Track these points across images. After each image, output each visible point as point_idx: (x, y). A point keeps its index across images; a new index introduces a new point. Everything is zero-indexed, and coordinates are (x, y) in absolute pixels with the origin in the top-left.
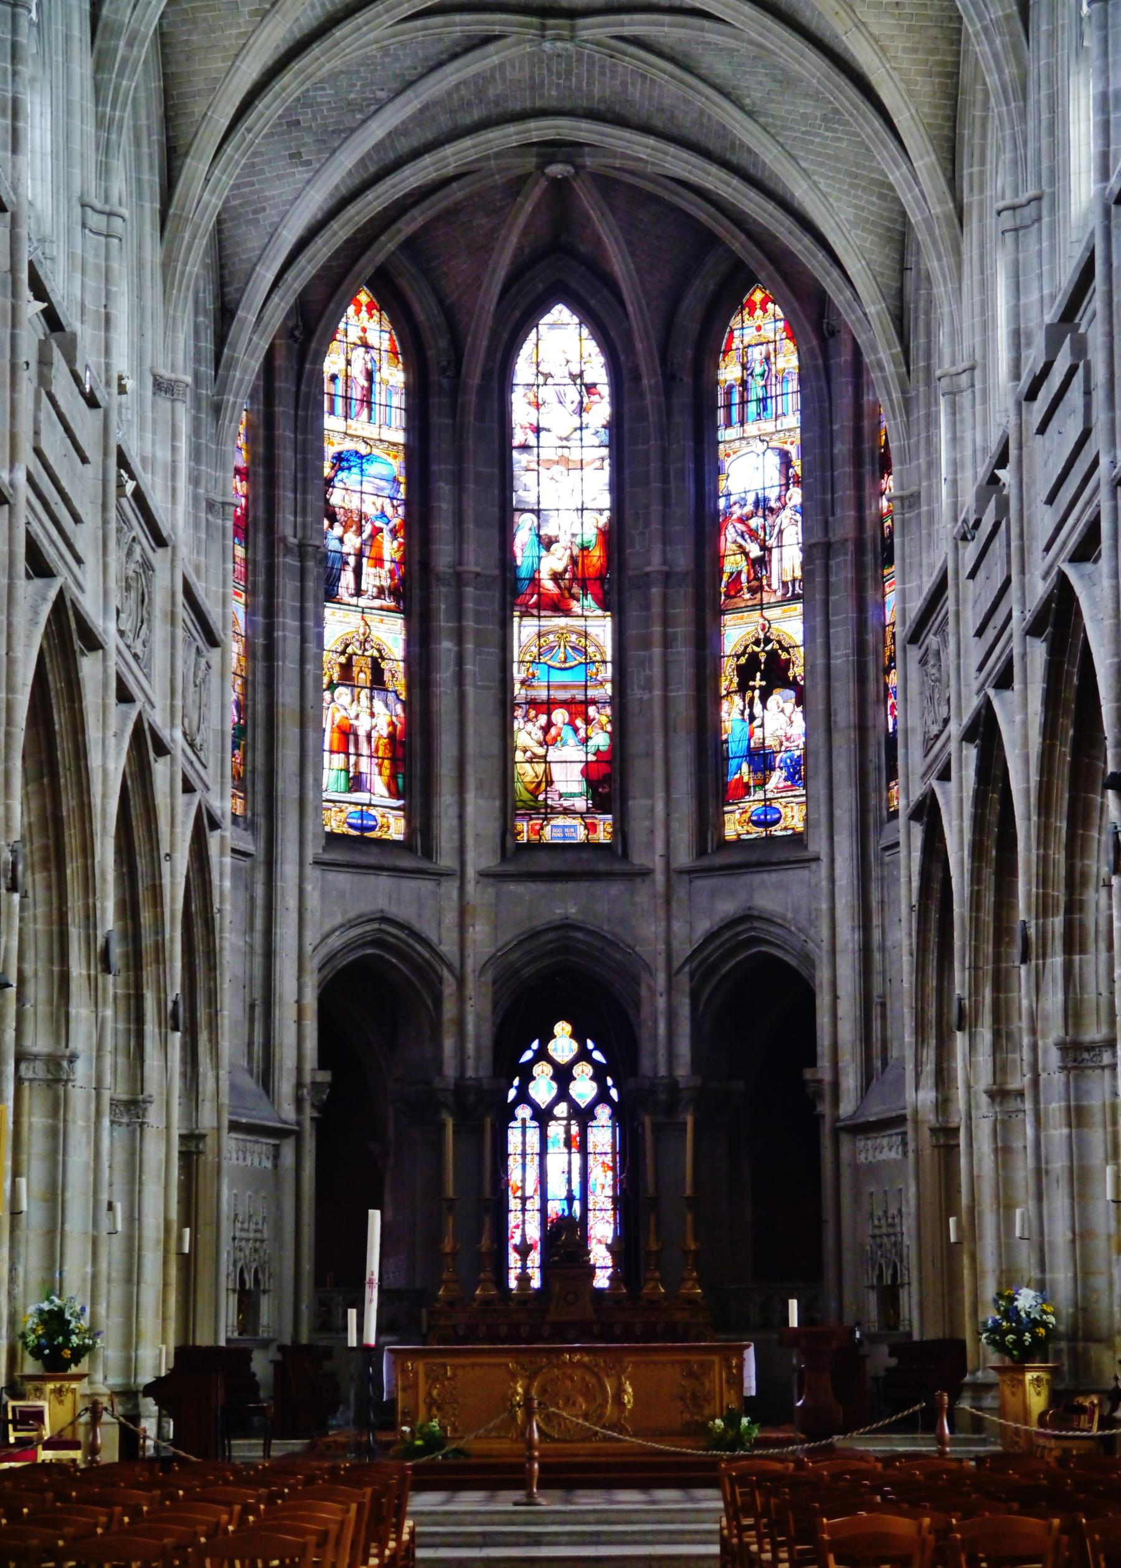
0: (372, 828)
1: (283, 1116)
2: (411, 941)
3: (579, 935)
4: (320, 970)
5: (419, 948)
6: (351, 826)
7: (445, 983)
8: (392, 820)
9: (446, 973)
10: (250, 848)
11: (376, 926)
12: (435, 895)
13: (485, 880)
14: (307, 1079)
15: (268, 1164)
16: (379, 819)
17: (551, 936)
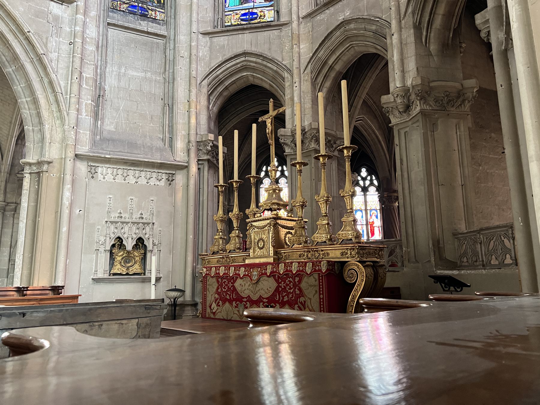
0: (256, 18)
1: (177, 159)
2: (265, 63)
3: (352, 26)
4: (208, 86)
5: (270, 65)
6: (242, 20)
7: (286, 80)
8: (266, 12)
9: (286, 75)
10: (165, 33)
11: (243, 59)
12: (279, 37)
13: (305, 20)
14: (193, 139)
15: (162, 183)
16: (259, 14)
17: (338, 33)
